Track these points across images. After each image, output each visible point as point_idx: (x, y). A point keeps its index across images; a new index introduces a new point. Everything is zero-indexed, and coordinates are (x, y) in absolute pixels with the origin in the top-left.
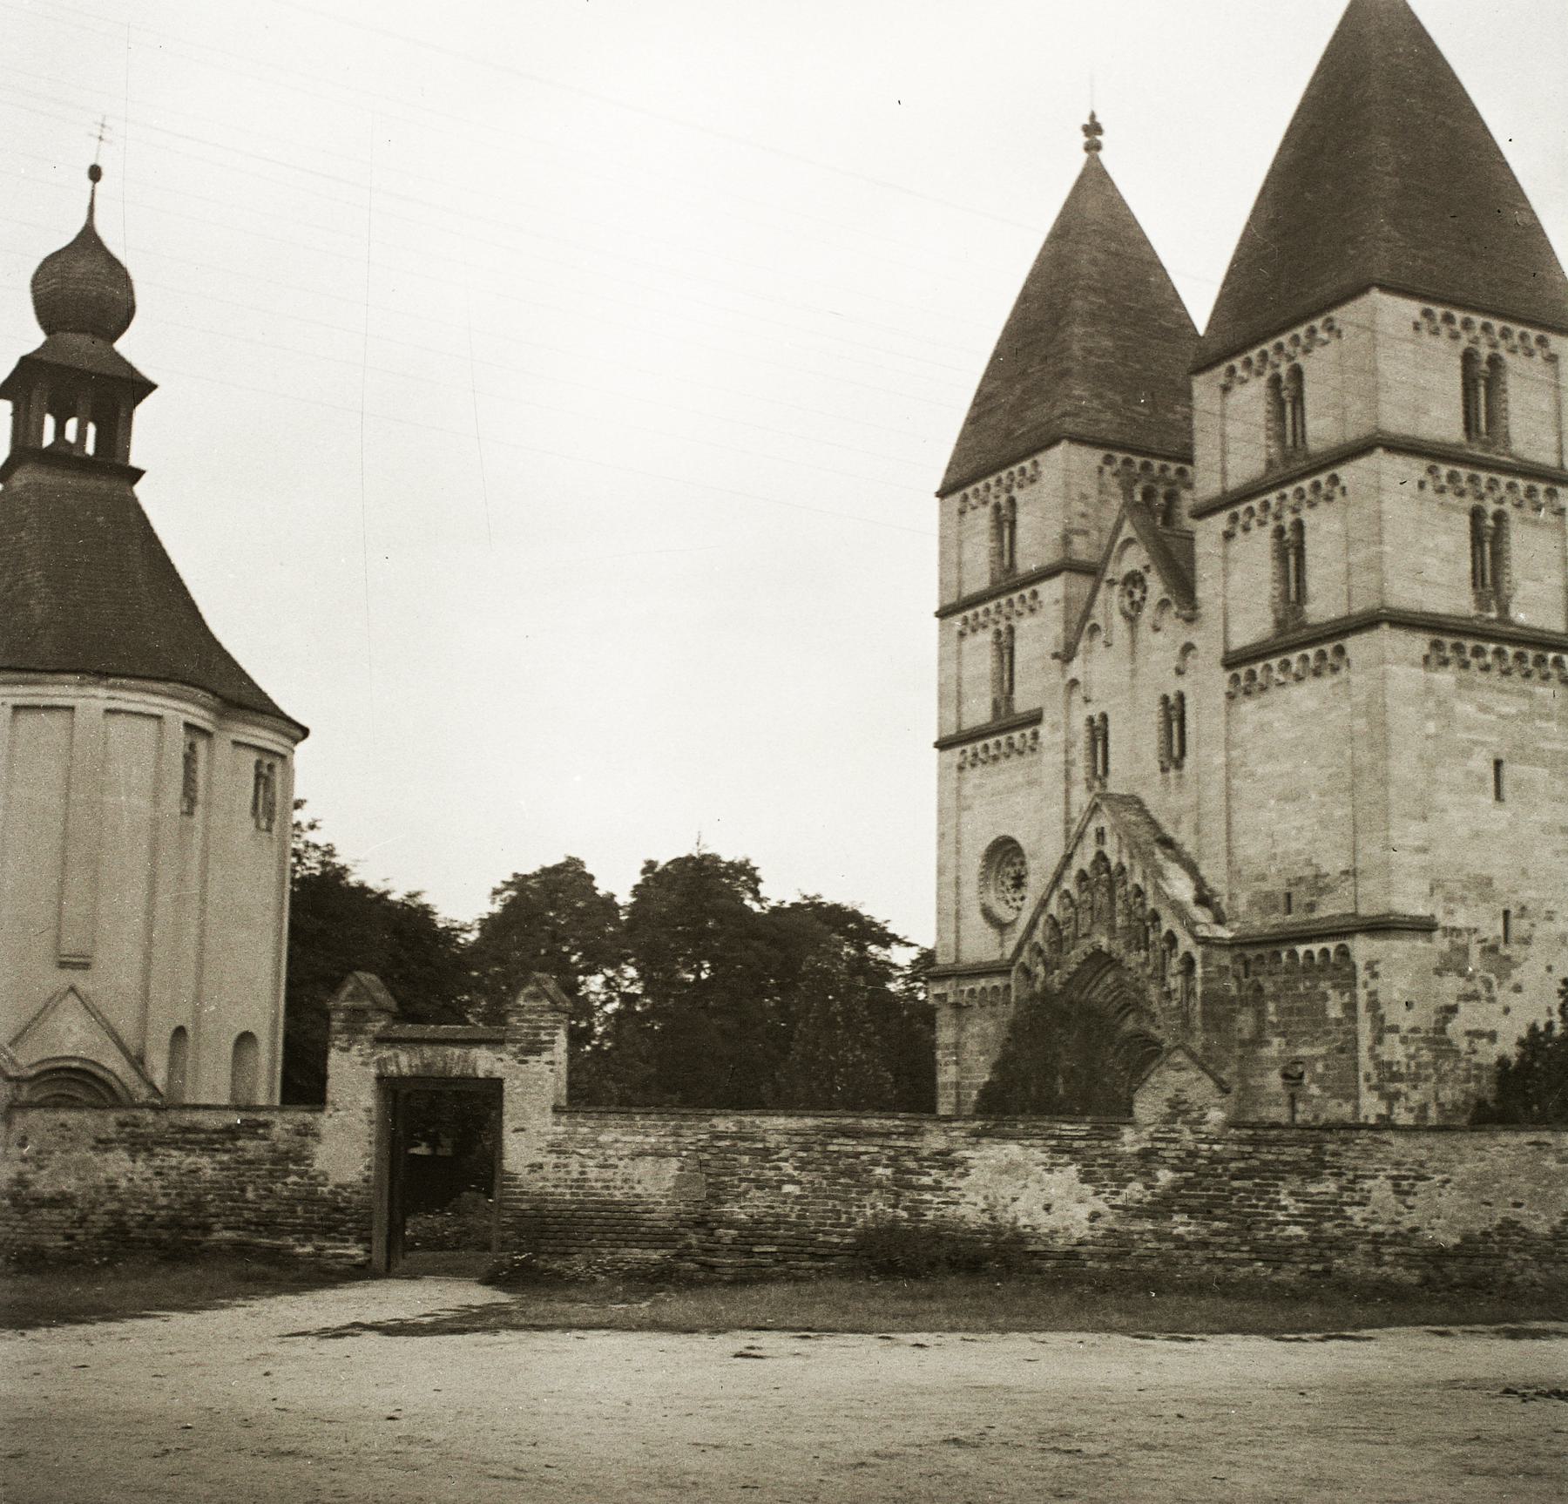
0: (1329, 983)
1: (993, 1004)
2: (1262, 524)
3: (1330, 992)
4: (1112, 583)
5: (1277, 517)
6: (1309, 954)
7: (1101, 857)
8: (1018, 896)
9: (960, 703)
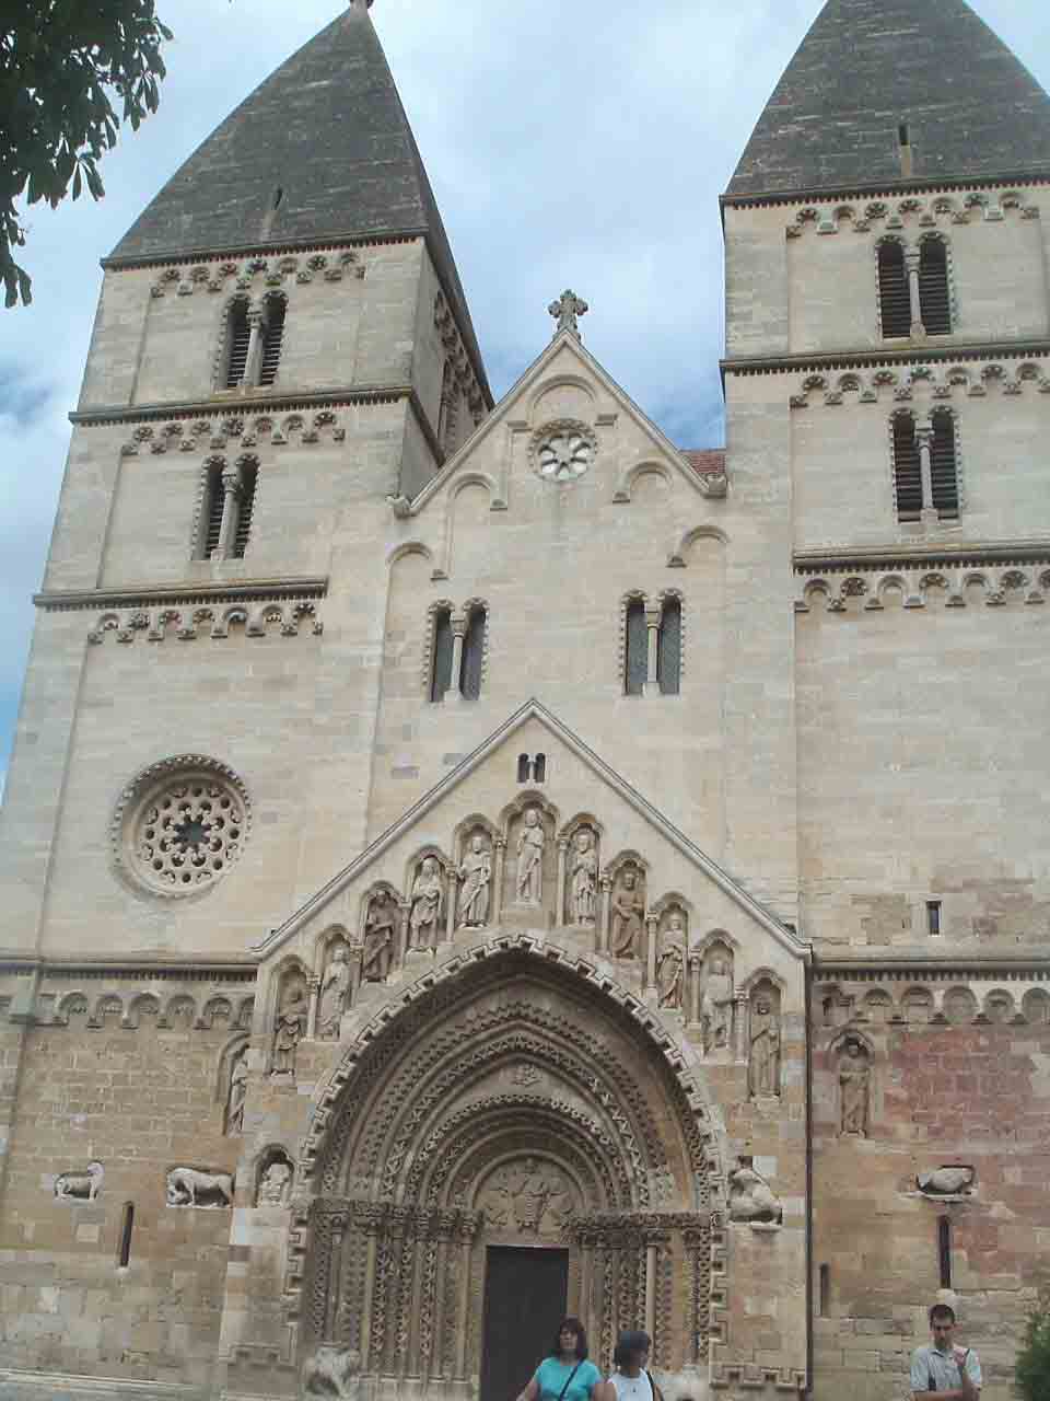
0: (1030, 1044)
1: (127, 1026)
2: (869, 399)
3: (1038, 1058)
4: (520, 427)
5: (904, 397)
6: (999, 1000)
7: (533, 801)
8: (190, 854)
9: (107, 544)
